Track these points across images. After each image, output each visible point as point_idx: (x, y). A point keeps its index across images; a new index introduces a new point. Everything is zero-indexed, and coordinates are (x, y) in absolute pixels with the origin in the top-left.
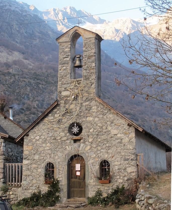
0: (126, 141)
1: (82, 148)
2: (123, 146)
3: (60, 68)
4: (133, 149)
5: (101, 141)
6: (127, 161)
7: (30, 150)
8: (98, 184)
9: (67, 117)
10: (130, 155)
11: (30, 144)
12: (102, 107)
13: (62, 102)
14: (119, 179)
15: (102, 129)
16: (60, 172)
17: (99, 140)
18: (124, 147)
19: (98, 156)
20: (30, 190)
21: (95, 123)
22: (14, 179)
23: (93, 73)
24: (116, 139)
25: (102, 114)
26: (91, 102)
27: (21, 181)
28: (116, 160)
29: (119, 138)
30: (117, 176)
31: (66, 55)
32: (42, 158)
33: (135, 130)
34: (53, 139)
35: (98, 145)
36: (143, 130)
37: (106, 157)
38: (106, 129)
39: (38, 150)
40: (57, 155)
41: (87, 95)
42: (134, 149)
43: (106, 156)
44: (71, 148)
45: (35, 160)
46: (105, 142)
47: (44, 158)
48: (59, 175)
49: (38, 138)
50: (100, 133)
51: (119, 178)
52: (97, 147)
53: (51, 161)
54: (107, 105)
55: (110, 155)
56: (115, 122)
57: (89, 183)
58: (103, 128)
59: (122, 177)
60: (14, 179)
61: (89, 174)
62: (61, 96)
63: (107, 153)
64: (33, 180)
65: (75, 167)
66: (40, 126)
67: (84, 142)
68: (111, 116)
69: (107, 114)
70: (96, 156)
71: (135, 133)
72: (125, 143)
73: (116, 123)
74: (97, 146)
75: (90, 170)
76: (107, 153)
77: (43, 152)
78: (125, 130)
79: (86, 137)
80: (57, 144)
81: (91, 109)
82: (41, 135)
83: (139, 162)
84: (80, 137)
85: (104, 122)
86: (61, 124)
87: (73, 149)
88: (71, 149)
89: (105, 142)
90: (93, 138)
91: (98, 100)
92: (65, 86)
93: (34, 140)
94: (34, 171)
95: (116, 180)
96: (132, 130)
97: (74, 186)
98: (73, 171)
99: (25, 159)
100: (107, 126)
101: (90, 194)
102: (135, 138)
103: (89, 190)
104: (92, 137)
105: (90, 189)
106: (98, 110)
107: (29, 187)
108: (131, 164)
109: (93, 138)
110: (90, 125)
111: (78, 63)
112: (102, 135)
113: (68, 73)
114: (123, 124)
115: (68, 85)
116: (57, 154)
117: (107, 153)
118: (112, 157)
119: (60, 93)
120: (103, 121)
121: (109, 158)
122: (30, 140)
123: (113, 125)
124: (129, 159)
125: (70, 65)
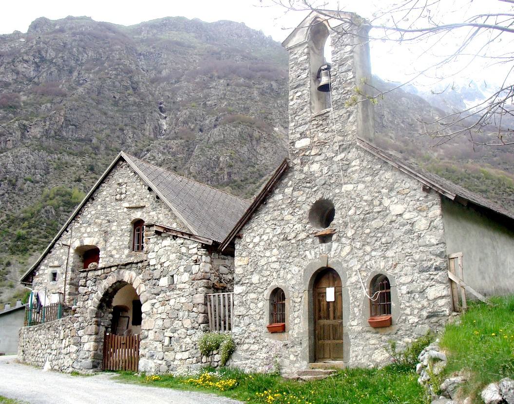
0: (422, 228)
1: (336, 253)
2: (415, 238)
3: (291, 97)
4: (437, 244)
5: (370, 232)
6: (426, 273)
7: (244, 266)
8: (367, 329)
9: (307, 191)
10: (432, 257)
11: (244, 254)
12: (370, 158)
13: (297, 161)
14: (411, 315)
15: (372, 207)
16: (296, 305)
17: (368, 231)
18: (420, 241)
19: (366, 267)
20: (245, 345)
21: (358, 195)
22: (222, 322)
23: (351, 91)
24: (401, 226)
25: (371, 174)
26: (349, 152)
27: (230, 329)
28: (402, 273)
29: (408, 221)
30: (406, 309)
31: (301, 69)
32: (265, 279)
33: (440, 199)
34: (283, 240)
35: (366, 243)
36: (457, 197)
37: (381, 266)
38: (380, 205)
39: (257, 263)
40: (290, 271)
41: (341, 138)
42: (441, 243)
43: (382, 264)
44: (315, 253)
45: (253, 285)
46: (380, 235)
47: (269, 280)
48: (295, 312)
49: (257, 240)
50: (368, 215)
51: (409, 313)
52: (364, 248)
53: (279, 284)
54: (378, 153)
55: (390, 263)
56: (397, 188)
57: (350, 328)
58: (374, 203)
59: (416, 312)
60: (222, 322)
61: (349, 308)
62: (294, 151)
63: (383, 258)
64: (250, 325)
65: (324, 294)
66: (261, 216)
67: (338, 240)
68: (388, 175)
69: (381, 172)
70: (361, 267)
71: (442, 207)
72: (419, 233)
73: (401, 189)
74: (363, 245)
75: (351, 298)
76: (385, 257)
77: (265, 267)
78: (418, 203)
79: (341, 227)
80: (290, 248)
81: (349, 167)
82: (263, 234)
83: (455, 275)
84: (331, 229)
85: (376, 190)
86: (297, 206)
87: (318, 257)
88: (315, 255)
89: (380, 235)
90: (355, 228)
91: (361, 146)
92: (301, 129)
93: (251, 246)
94: (251, 307)
95: (404, 318)
96: (435, 199)
97: (324, 336)
98: (322, 303)
99: (237, 284)
100: (382, 198)
101: (353, 351)
102: (443, 217)
103: (350, 342)
104: (352, 226)
105: (352, 340)
106: (363, 166)
107: (243, 340)
108: (435, 278)
109: (355, 228)
110: (349, 201)
111: (324, 80)
112: (372, 221)
113: (305, 103)
114: (415, 190)
115: (307, 126)
116: (289, 269)
117: (385, 257)
118: (395, 265)
119: (292, 144)
120: (372, 189)
121: (387, 270)
122: (244, 245)
123: (393, 194)
124: (430, 268)
125: (309, 86)
